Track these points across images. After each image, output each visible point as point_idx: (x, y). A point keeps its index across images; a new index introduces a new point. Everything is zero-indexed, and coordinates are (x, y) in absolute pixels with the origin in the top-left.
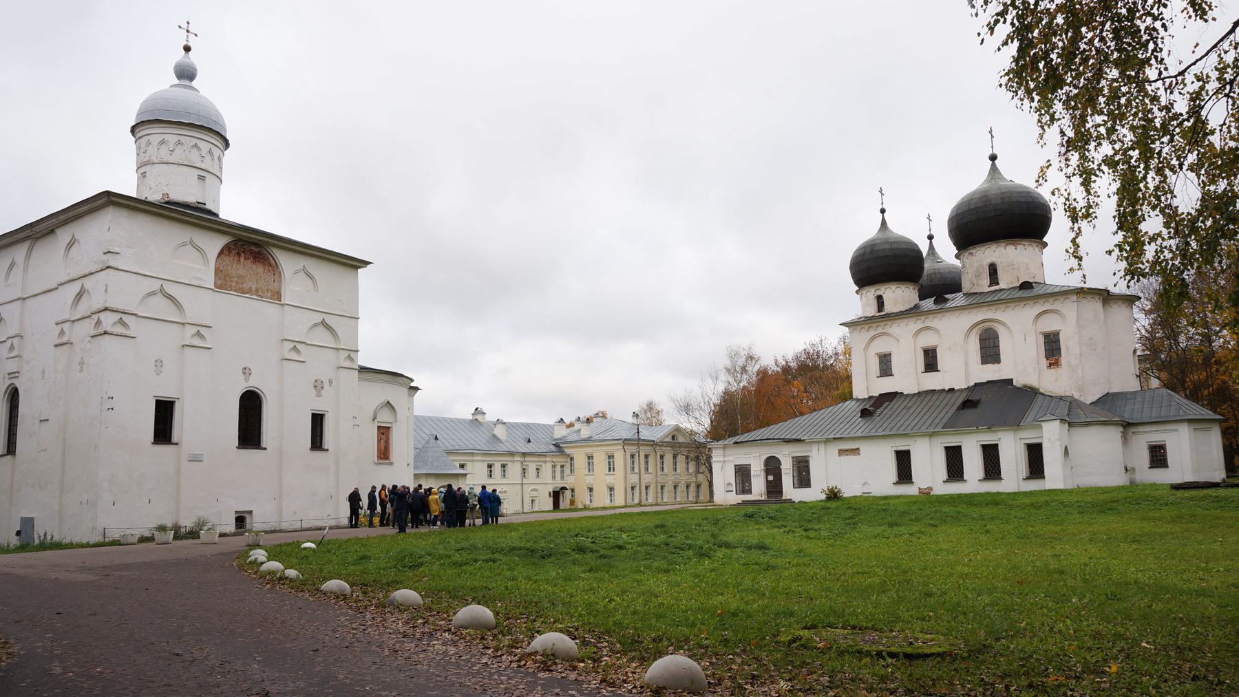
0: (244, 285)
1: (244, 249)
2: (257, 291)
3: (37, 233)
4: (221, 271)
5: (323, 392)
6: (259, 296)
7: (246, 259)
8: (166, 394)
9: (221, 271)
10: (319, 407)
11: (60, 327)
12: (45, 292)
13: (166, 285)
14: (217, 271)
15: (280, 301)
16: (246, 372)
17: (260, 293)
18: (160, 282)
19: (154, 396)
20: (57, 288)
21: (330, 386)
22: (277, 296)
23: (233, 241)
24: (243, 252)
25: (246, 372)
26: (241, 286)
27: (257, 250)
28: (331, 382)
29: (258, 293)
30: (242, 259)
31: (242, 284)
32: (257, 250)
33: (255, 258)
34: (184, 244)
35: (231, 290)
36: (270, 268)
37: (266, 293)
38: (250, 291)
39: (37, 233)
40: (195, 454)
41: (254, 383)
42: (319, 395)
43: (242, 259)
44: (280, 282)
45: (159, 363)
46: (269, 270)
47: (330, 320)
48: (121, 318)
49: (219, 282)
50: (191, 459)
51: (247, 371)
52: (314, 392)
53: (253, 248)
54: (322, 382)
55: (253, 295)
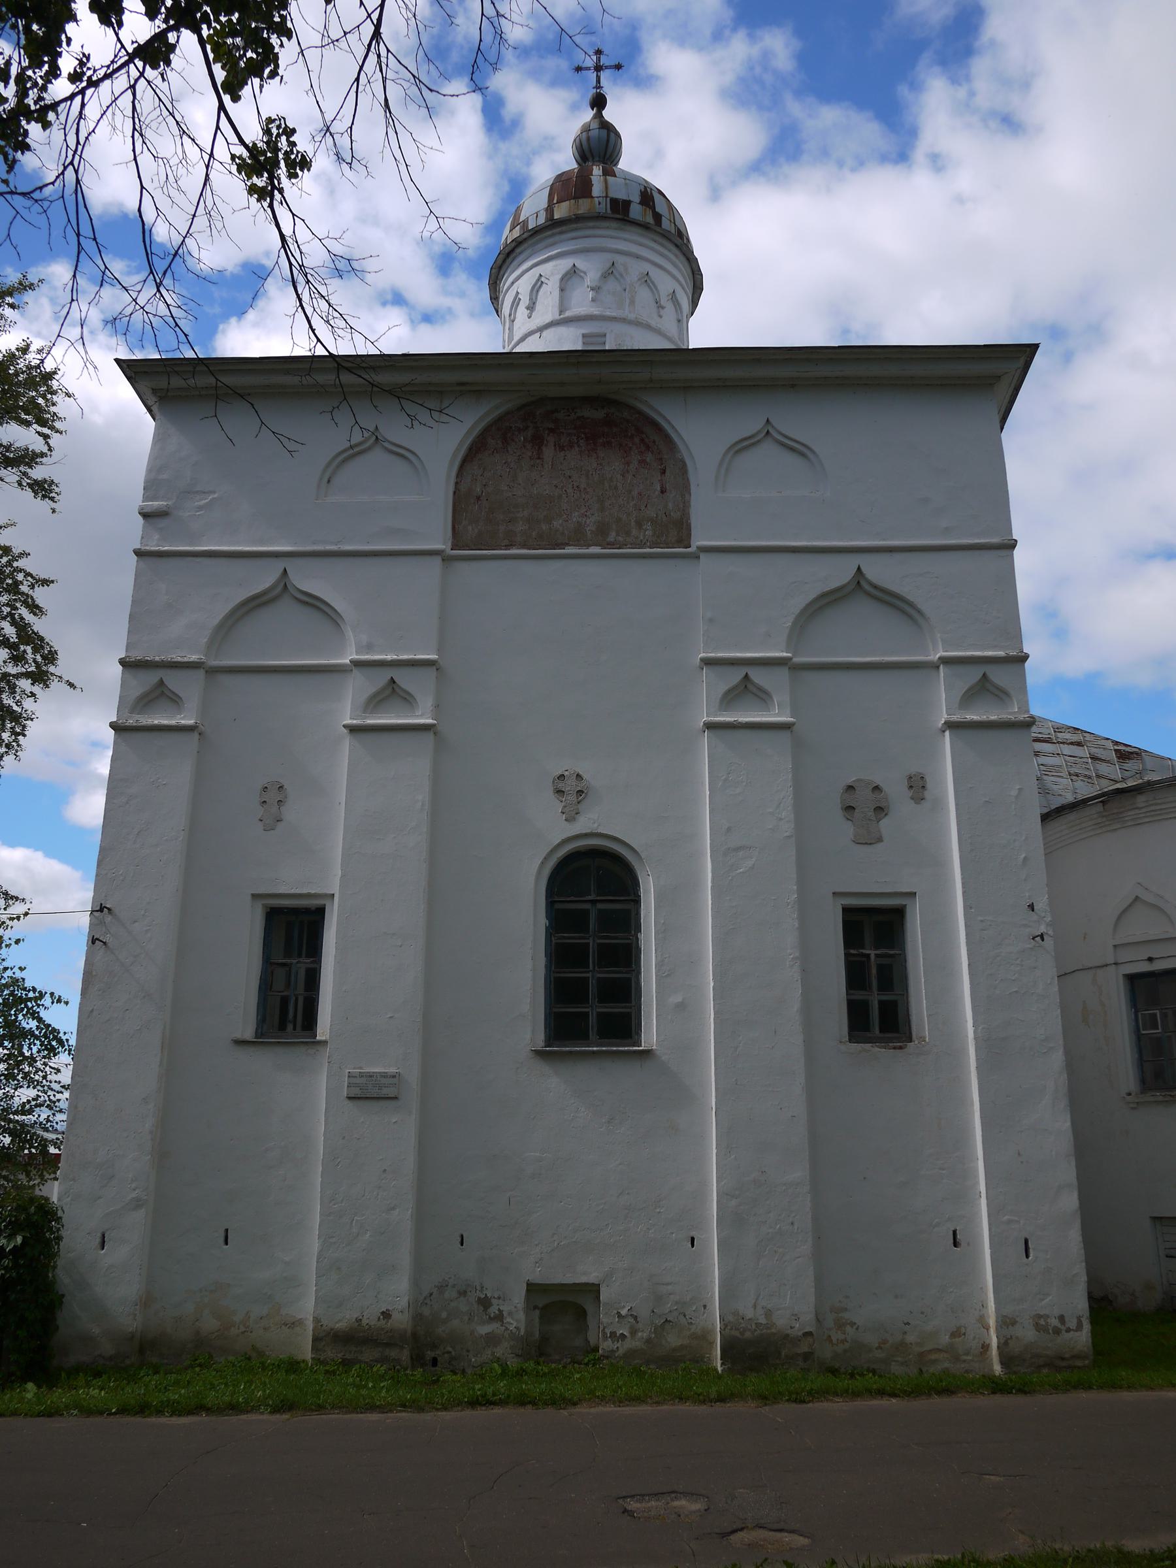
0: (556, 524)
4: (478, 498)
5: (886, 825)
6: (611, 545)
7: (562, 448)
9: (478, 498)
13: (292, 566)
17: (612, 537)
18: (278, 566)
19: (255, 897)
24: (551, 431)
26: (544, 527)
28: (918, 786)
32: (600, 414)
34: (353, 453)
35: (507, 547)
36: (649, 457)
37: (634, 532)
38: (578, 537)
40: (370, 1076)
43: (548, 452)
44: (685, 488)
46: (642, 462)
47: (878, 571)
50: (356, 1092)
51: (570, 785)
52: (848, 830)
53: (588, 413)
54: (877, 788)
55: (588, 546)
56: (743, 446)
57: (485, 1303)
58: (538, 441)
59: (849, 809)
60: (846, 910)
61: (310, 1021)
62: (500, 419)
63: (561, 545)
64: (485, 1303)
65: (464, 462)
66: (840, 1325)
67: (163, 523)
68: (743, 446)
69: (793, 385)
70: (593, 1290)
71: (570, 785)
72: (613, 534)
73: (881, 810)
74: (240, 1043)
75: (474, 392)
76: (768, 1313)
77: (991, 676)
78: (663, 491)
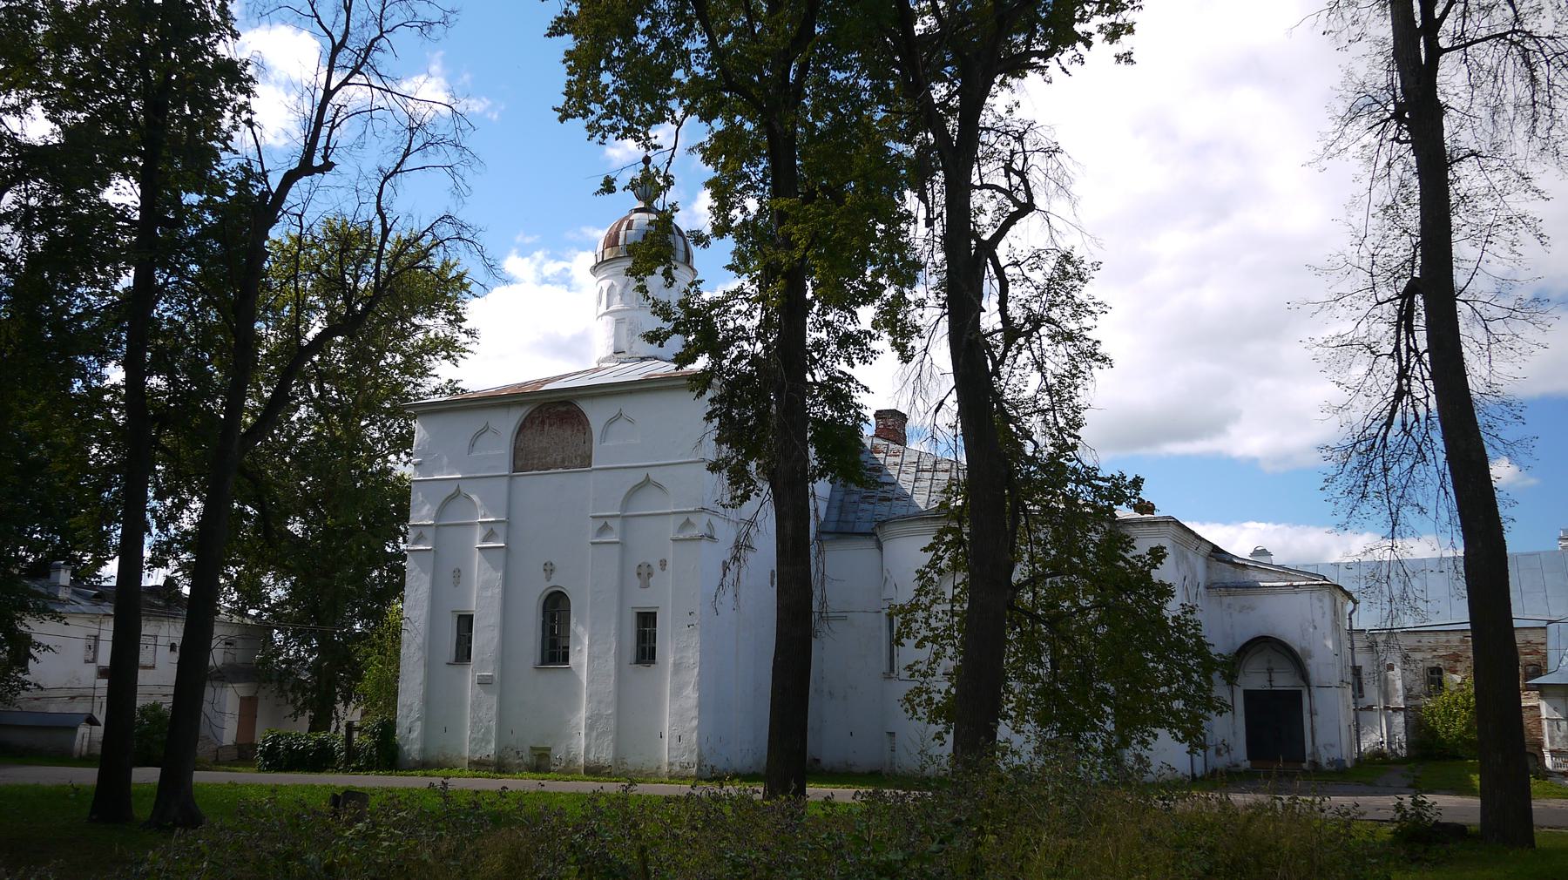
2: (563, 461)
10: (645, 602)
16: (549, 569)
21: (663, 569)
25: (549, 569)
27: (564, 409)
28: (663, 564)
29: (564, 464)
31: (545, 457)
32: (564, 409)
36: (581, 428)
41: (559, 581)
42: (645, 585)
43: (546, 427)
49: (520, 463)
52: (638, 582)
56: (611, 422)
57: (518, 753)
58: (543, 422)
59: (639, 574)
60: (639, 614)
61: (469, 657)
62: (530, 414)
63: (549, 469)
64: (518, 753)
65: (518, 434)
66: (622, 764)
67: (420, 467)
68: (611, 422)
69: (631, 392)
70: (549, 749)
71: (548, 568)
73: (650, 575)
74: (448, 664)
75: (521, 404)
76: (598, 758)
77: (691, 519)
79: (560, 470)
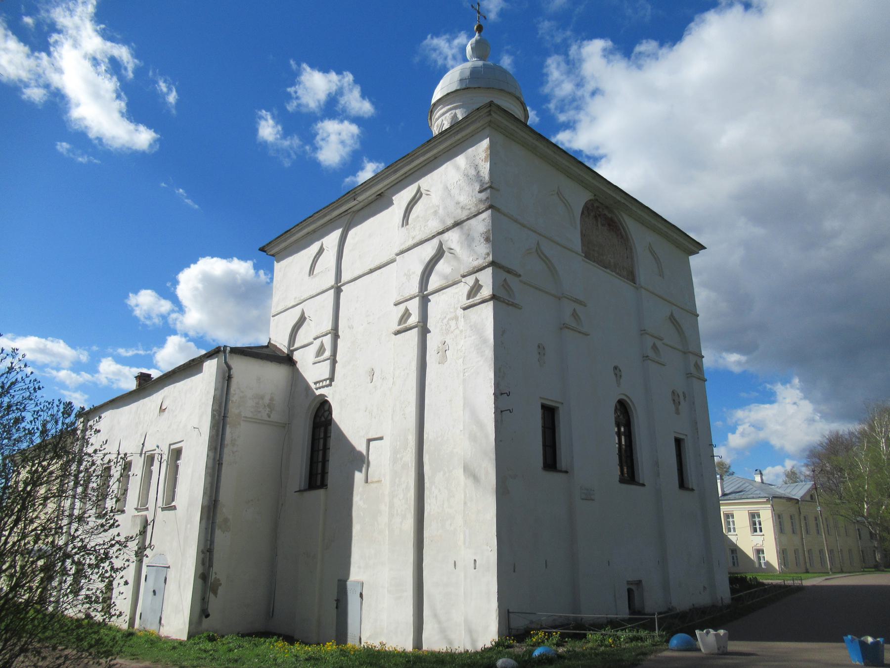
1: (600, 212)
3: (360, 202)
6: (617, 274)
8: (552, 397)
11: (402, 308)
12: (371, 271)
14: (583, 235)
15: (635, 284)
19: (541, 398)
20: (393, 261)
22: (631, 277)
23: (590, 200)
30: (599, 225)
33: (609, 225)
35: (594, 261)
39: (360, 202)
45: (541, 349)
48: (505, 280)
55: (613, 272)
63: (606, 268)
72: (618, 270)
78: (627, 258)
79: (614, 273)
